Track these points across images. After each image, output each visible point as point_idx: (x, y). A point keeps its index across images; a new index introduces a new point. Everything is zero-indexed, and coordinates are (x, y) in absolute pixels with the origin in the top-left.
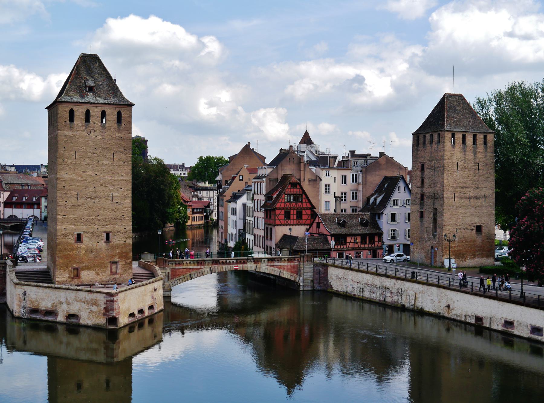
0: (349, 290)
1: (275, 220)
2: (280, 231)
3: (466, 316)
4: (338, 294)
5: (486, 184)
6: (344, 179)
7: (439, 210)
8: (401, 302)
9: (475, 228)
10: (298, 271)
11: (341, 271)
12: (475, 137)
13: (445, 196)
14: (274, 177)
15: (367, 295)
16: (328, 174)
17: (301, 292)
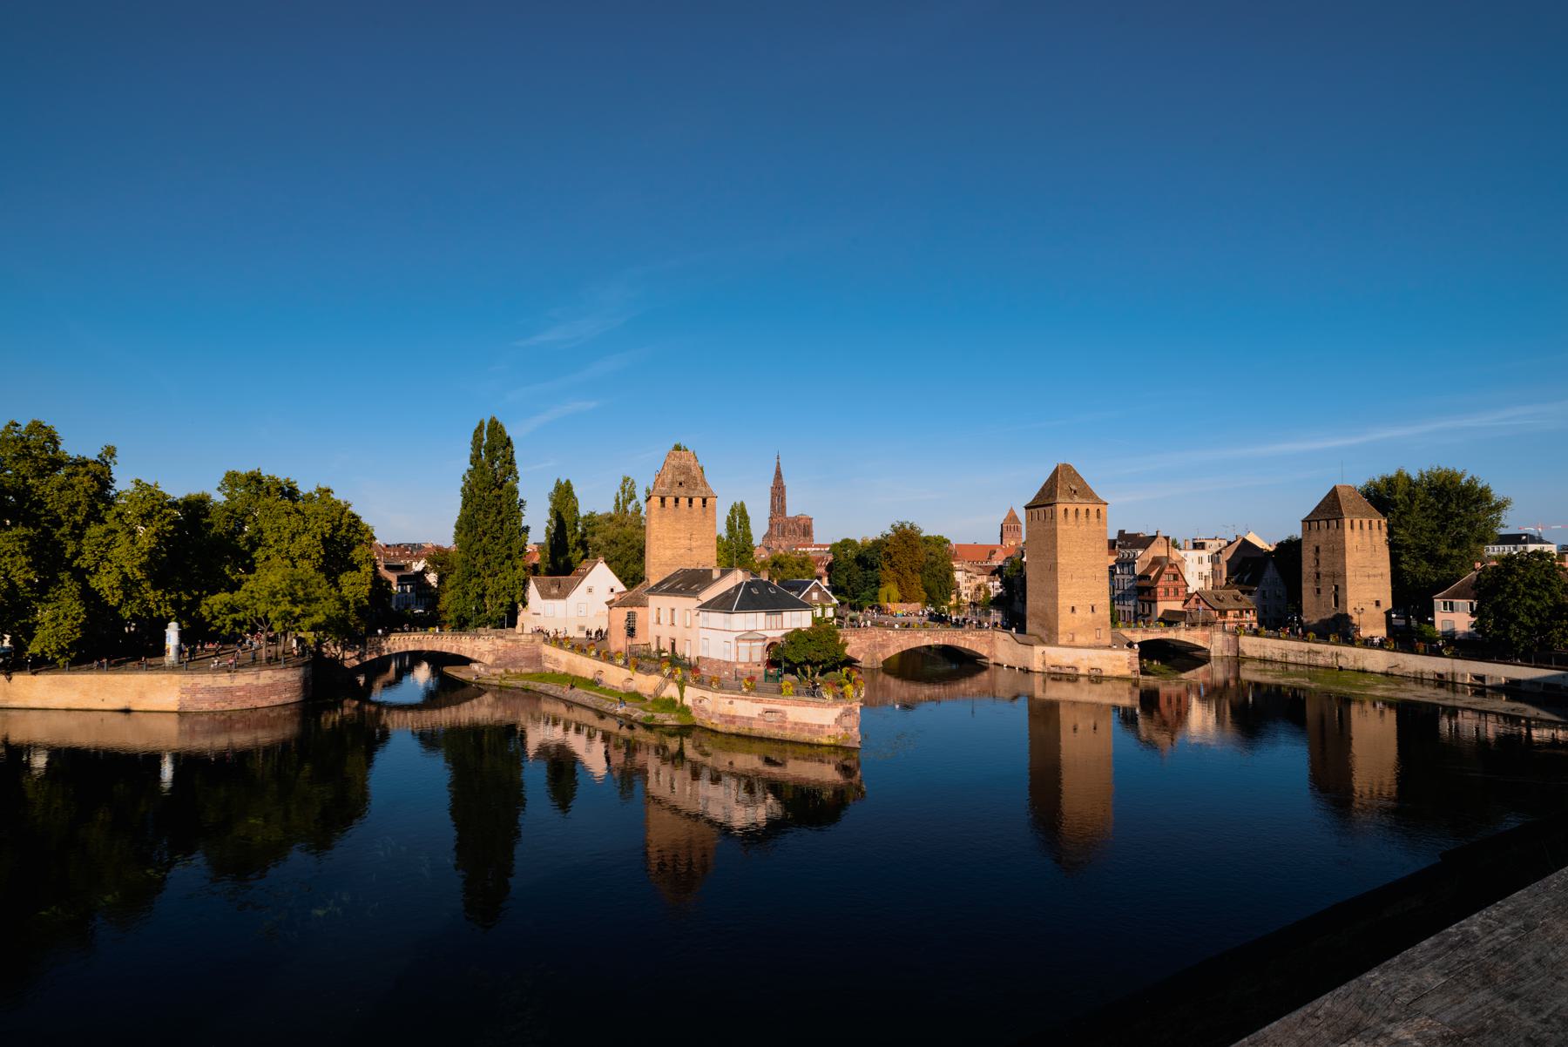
0: (1268, 654)
1: (1156, 596)
2: (1162, 606)
3: (1422, 673)
4: (1252, 659)
5: (1383, 564)
6: (1200, 560)
7: (1341, 586)
8: (1337, 664)
9: (1374, 603)
10: (1209, 639)
11: (1256, 640)
12: (1370, 522)
13: (1347, 574)
14: (1145, 558)
15: (1291, 659)
16: (1186, 555)
17: (1212, 658)
